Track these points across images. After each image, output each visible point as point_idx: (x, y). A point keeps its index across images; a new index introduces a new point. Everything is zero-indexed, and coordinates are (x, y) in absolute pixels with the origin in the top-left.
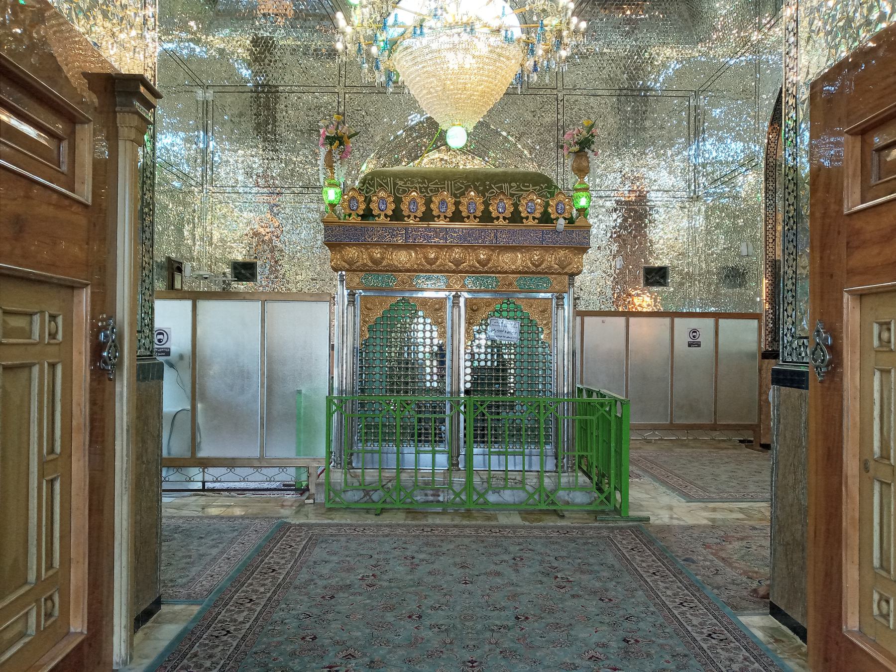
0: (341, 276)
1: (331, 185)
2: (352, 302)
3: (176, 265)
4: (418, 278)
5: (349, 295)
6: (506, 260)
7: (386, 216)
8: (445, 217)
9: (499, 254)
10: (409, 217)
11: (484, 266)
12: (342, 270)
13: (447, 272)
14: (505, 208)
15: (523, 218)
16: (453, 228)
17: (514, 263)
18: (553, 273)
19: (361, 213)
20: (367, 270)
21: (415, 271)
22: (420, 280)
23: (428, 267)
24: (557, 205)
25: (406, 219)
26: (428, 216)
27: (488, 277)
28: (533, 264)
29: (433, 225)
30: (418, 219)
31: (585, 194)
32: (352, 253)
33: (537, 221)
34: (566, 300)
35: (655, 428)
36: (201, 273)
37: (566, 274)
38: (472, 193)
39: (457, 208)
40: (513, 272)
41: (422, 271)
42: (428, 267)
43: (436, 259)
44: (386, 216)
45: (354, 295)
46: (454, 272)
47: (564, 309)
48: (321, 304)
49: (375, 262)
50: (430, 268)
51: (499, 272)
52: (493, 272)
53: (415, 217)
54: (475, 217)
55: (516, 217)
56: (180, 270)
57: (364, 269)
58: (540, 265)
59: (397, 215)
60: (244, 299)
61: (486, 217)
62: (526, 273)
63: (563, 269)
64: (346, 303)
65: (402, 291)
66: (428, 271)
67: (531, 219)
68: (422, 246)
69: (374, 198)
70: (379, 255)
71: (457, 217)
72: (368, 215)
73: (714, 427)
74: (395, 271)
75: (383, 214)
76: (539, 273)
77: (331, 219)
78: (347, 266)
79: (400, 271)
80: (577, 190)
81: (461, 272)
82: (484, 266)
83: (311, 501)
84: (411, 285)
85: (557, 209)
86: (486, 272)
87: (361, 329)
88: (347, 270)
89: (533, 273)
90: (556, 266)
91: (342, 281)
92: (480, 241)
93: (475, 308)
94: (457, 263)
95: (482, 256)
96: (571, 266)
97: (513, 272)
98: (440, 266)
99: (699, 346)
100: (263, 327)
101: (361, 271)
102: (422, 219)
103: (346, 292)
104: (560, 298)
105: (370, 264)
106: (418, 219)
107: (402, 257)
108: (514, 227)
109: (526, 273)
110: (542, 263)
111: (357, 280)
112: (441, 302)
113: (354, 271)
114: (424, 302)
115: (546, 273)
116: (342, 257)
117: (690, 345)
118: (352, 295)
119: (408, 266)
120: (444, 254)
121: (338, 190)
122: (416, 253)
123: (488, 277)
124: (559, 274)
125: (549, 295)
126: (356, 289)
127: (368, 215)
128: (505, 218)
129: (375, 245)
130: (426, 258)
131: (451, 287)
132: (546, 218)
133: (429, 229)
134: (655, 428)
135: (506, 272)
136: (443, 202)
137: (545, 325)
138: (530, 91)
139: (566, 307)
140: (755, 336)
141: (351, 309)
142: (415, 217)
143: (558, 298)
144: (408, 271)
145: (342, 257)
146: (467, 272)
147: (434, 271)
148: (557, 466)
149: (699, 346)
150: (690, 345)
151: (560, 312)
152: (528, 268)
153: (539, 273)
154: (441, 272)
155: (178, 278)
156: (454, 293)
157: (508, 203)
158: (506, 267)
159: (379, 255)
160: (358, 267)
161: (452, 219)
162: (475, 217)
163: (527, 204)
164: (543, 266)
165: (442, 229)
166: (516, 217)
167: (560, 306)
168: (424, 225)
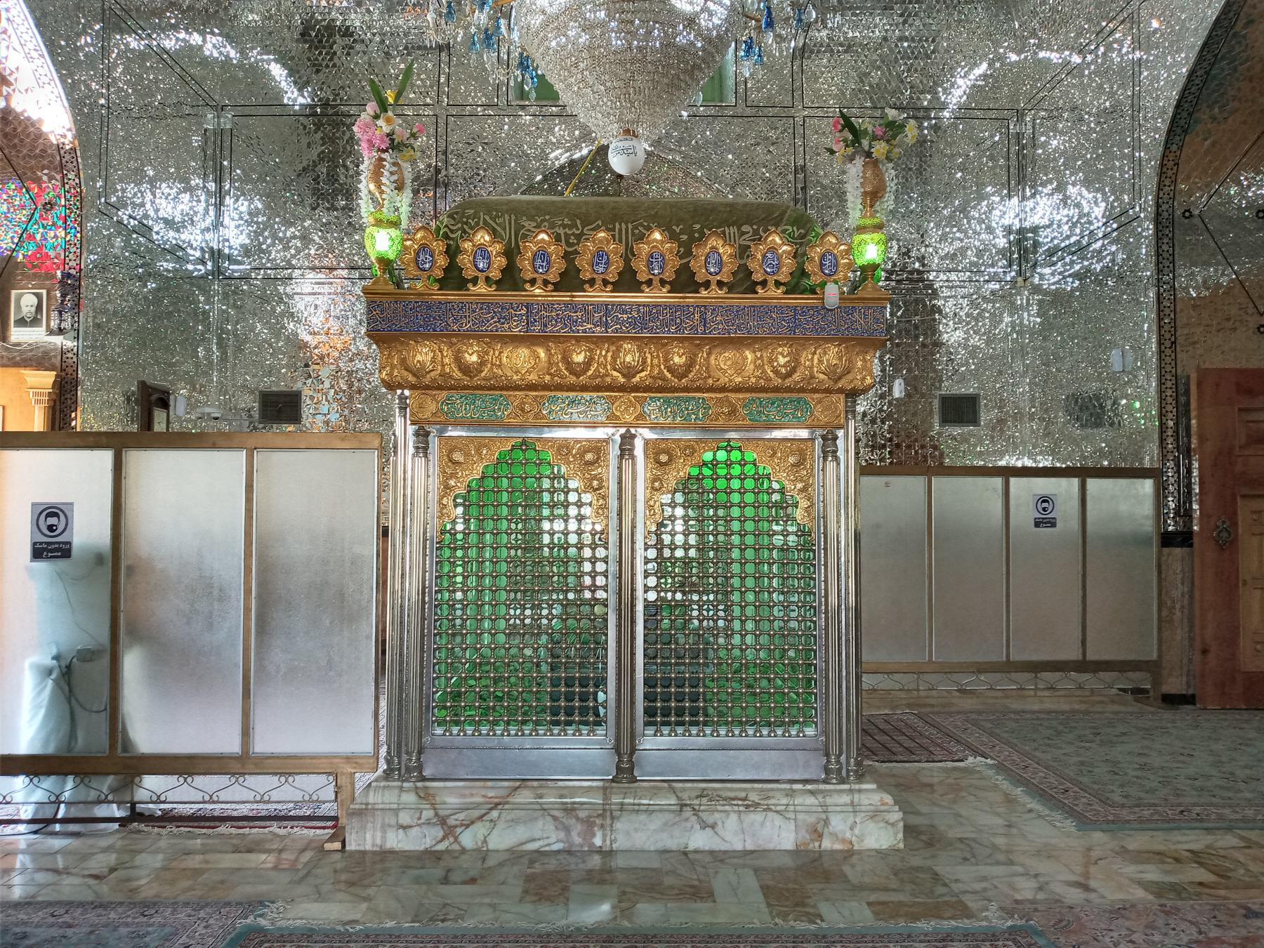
0: (402, 398)
1: (378, 223)
2: (423, 449)
3: (154, 397)
4: (553, 400)
5: (417, 434)
6: (727, 365)
8: (605, 282)
9: (709, 354)
10: (533, 282)
11: (680, 377)
13: (610, 388)
14: (720, 264)
15: (757, 283)
16: (621, 304)
17: (740, 371)
18: (815, 391)
19: (440, 274)
20: (450, 388)
21: (546, 387)
22: (557, 406)
23: (572, 379)
24: (823, 257)
25: (527, 286)
26: (570, 280)
27: (688, 400)
28: (776, 372)
29: (580, 297)
30: (550, 287)
31: (877, 236)
32: (423, 355)
33: (782, 289)
34: (840, 443)
35: (981, 668)
36: (208, 410)
37: (841, 391)
38: (657, 236)
40: (738, 389)
41: (559, 388)
42: (572, 379)
43: (588, 364)
45: (427, 434)
46: (622, 389)
47: (836, 459)
48: (359, 454)
49: (465, 369)
50: (579, 384)
51: (711, 389)
52: (698, 390)
53: (546, 282)
54: (663, 283)
55: (744, 282)
56: (164, 404)
57: (443, 385)
58: (789, 375)
59: (510, 278)
60: (214, 447)
61: (685, 281)
62: (763, 390)
63: (836, 381)
64: (411, 450)
65: (522, 427)
66: (571, 388)
67: (771, 284)
68: (557, 339)
69: (467, 245)
70: (474, 358)
71: (628, 281)
72: (453, 278)
73: (1083, 666)
74: (507, 388)
76: (789, 390)
77: (381, 288)
78: (411, 378)
79: (517, 388)
80: (861, 229)
81: (636, 389)
83: (337, 845)
84: (538, 416)
85: (821, 265)
86: (686, 389)
87: (440, 502)
88: (413, 387)
89: (776, 390)
90: (822, 376)
91: (403, 409)
92: (673, 329)
93: (664, 458)
94: (629, 372)
95: (677, 359)
96: (850, 377)
97: (738, 389)
98: (592, 377)
99: (1053, 525)
100: (249, 500)
101: (440, 388)
102: (557, 287)
103: (411, 429)
104: (829, 440)
105: (457, 374)
106: (550, 287)
107: (520, 361)
108: (740, 300)
109: (763, 390)
110: (793, 370)
111: (432, 407)
112: (598, 448)
113: (427, 387)
114: (563, 448)
115: (802, 390)
116: (403, 361)
117: (1037, 524)
118: (422, 435)
119: (533, 378)
120: (604, 354)
121: (394, 233)
122: (548, 350)
123: (688, 400)
124: (828, 391)
125: (804, 434)
126: (429, 423)
127: (453, 278)
128: (720, 284)
129: (466, 337)
130: (567, 360)
131: (617, 418)
132: (797, 283)
133: (573, 306)
134: (981, 668)
135: (723, 389)
136: (600, 254)
137: (801, 491)
138: (749, 111)
139: (841, 454)
140: (1148, 508)
141: (421, 462)
142: (546, 282)
143: (824, 438)
144: (532, 387)
145: (403, 361)
146: (648, 389)
147: (584, 388)
148: (827, 771)
149: (1053, 525)
150: (1037, 524)
151: (831, 465)
152: (769, 380)
153: (789, 390)
154: (597, 389)
155: (159, 417)
156: (623, 430)
157: (725, 251)
158: (724, 380)
159: (474, 358)
160: (434, 380)
161: (617, 287)
162: (663, 283)
163: (764, 256)
164: (796, 377)
165: (597, 307)
166: (744, 282)
167: (829, 451)
168: (564, 297)
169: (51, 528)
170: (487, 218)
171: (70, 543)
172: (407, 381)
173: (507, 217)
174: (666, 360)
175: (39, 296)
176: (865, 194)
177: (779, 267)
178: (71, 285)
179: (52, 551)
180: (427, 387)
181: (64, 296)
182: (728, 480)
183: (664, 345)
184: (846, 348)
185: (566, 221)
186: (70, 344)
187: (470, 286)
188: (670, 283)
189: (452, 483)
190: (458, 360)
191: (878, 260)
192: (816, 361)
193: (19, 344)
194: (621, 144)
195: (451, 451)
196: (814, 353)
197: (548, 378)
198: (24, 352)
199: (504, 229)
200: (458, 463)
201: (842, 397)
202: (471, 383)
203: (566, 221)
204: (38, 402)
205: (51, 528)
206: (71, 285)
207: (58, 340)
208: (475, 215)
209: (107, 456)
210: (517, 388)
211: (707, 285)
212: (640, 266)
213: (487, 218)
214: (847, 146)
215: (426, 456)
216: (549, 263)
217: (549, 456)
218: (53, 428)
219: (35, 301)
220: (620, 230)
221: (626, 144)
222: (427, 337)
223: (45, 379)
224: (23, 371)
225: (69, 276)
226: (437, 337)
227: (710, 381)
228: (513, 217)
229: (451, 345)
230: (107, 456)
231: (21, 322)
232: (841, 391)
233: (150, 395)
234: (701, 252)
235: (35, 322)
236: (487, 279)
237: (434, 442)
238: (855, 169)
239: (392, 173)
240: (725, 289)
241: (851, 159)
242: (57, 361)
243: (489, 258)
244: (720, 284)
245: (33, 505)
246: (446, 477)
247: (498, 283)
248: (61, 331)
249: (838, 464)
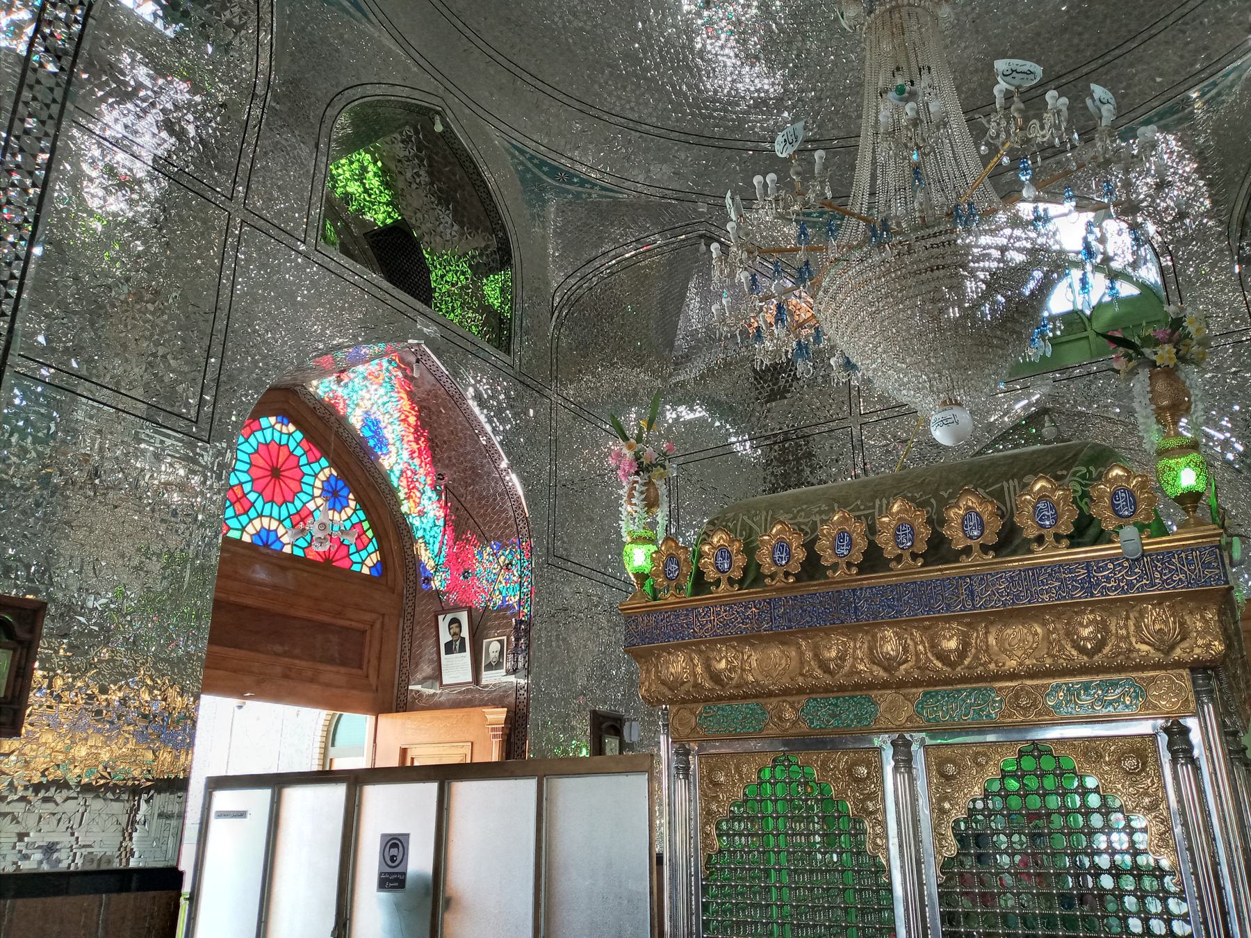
0: (666, 713)
7: (731, 581)
12: (660, 702)
23: (828, 680)
32: (677, 666)
34: (1195, 737)
37: (1178, 664)
39: (872, 544)
44: (731, 581)
47: (1193, 762)
54: (914, 556)
56: (617, 730)
75: (724, 578)
79: (771, 694)
80: (1163, 453)
82: (952, 665)
86: (964, 680)
88: (671, 702)
93: (950, 769)
124: (1158, 666)
128: (985, 549)
135: (1013, 676)
169: (393, 859)
170: (745, 518)
171: (404, 874)
172: (665, 697)
173: (764, 513)
174: (933, 646)
175: (501, 642)
176: (1159, 413)
177: (1056, 518)
178: (523, 630)
179: (392, 881)
180: (684, 701)
181: (517, 640)
182: (1005, 798)
183: (929, 628)
184: (1171, 607)
185: (824, 507)
186: (523, 682)
187: (713, 588)
188: (922, 555)
189: (714, 807)
190: (708, 667)
191: (1201, 487)
192: (1132, 628)
193: (487, 686)
194: (939, 416)
195: (711, 771)
196: (1127, 618)
197: (800, 680)
198: (491, 692)
199: (760, 527)
200: (717, 784)
201: (1185, 673)
202: (718, 694)
203: (824, 507)
204: (495, 736)
205: (393, 859)
206: (523, 630)
207: (512, 679)
208: (735, 518)
209: (433, 787)
210: (771, 694)
211: (967, 551)
212: (884, 539)
213: (745, 518)
214: (1130, 360)
215: (687, 777)
216: (789, 554)
217: (1071, 761)
218: (508, 757)
219: (499, 645)
220: (881, 506)
221: (948, 414)
222: (678, 647)
223: (498, 715)
224: (486, 710)
225: (521, 622)
226: (686, 646)
227: (992, 666)
228: (770, 512)
229: (700, 652)
230: (433, 787)
231: (490, 667)
232: (1178, 664)
233: (601, 723)
234: (955, 514)
235: (498, 665)
236: (729, 578)
237: (694, 761)
238: (1140, 383)
239: (642, 493)
240: (991, 554)
241: (1132, 373)
242: (512, 699)
243: (730, 557)
244: (985, 549)
245: (383, 836)
246: (708, 798)
247: (741, 582)
248: (515, 671)
249: (1197, 769)
